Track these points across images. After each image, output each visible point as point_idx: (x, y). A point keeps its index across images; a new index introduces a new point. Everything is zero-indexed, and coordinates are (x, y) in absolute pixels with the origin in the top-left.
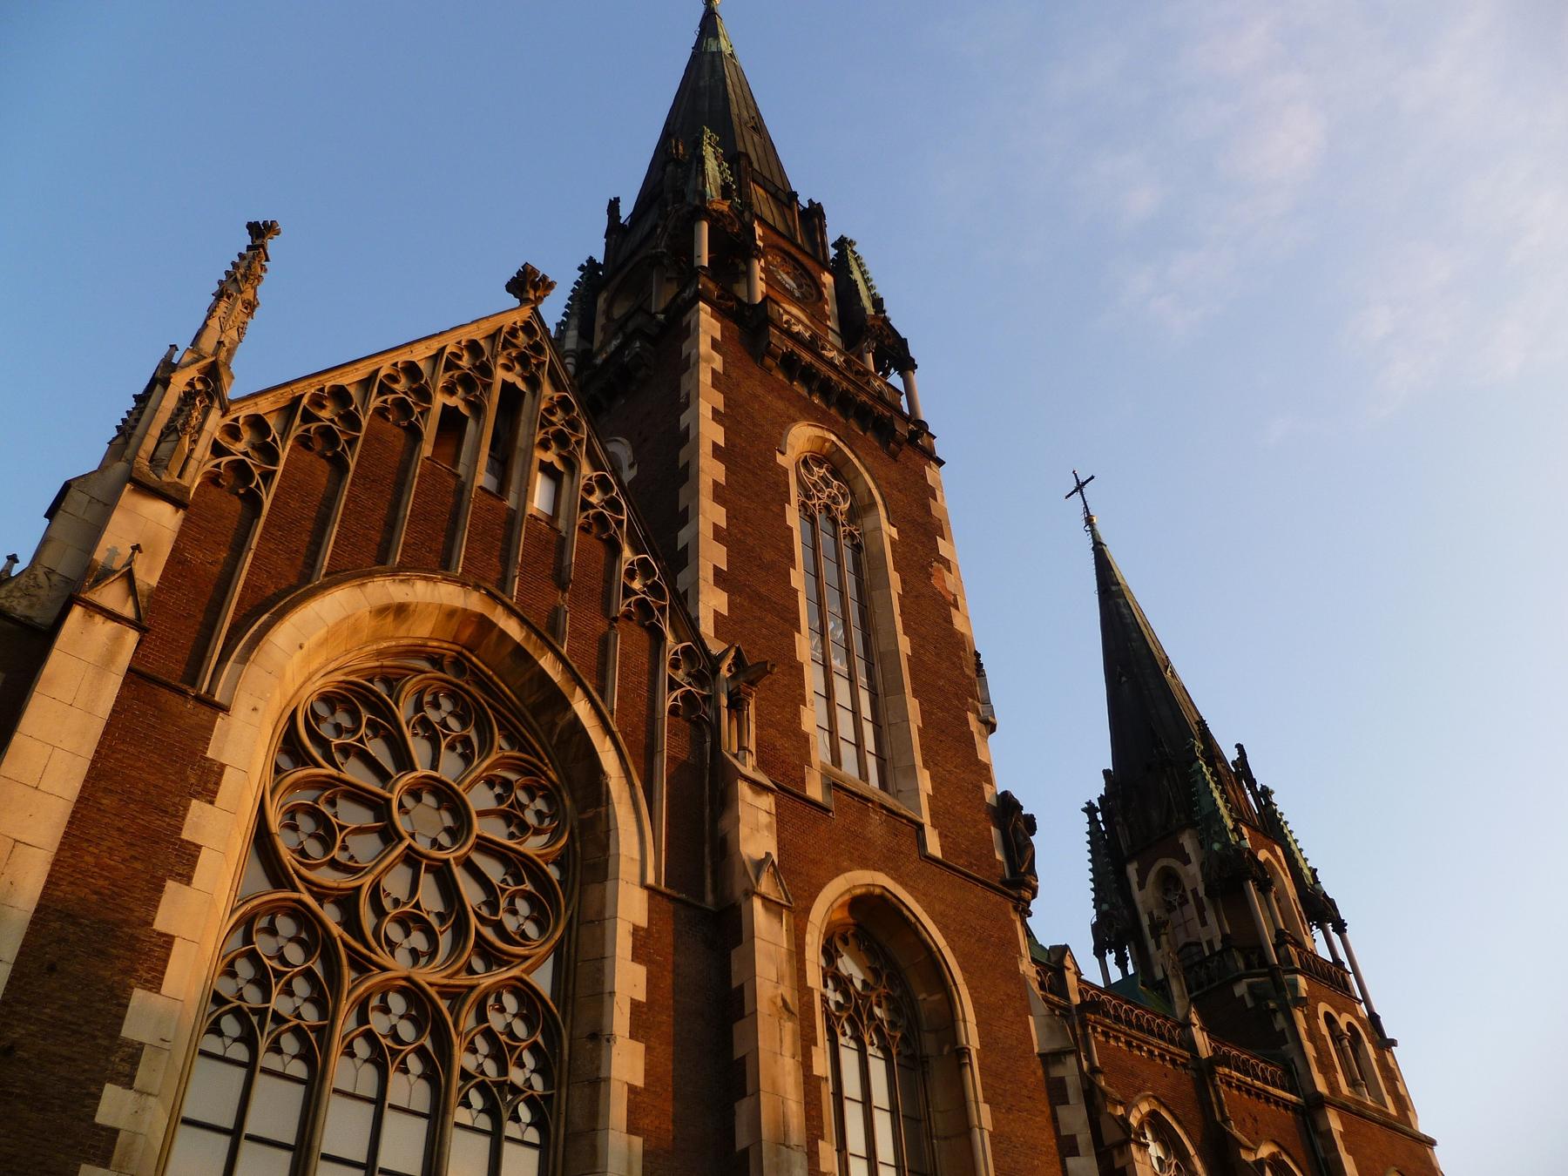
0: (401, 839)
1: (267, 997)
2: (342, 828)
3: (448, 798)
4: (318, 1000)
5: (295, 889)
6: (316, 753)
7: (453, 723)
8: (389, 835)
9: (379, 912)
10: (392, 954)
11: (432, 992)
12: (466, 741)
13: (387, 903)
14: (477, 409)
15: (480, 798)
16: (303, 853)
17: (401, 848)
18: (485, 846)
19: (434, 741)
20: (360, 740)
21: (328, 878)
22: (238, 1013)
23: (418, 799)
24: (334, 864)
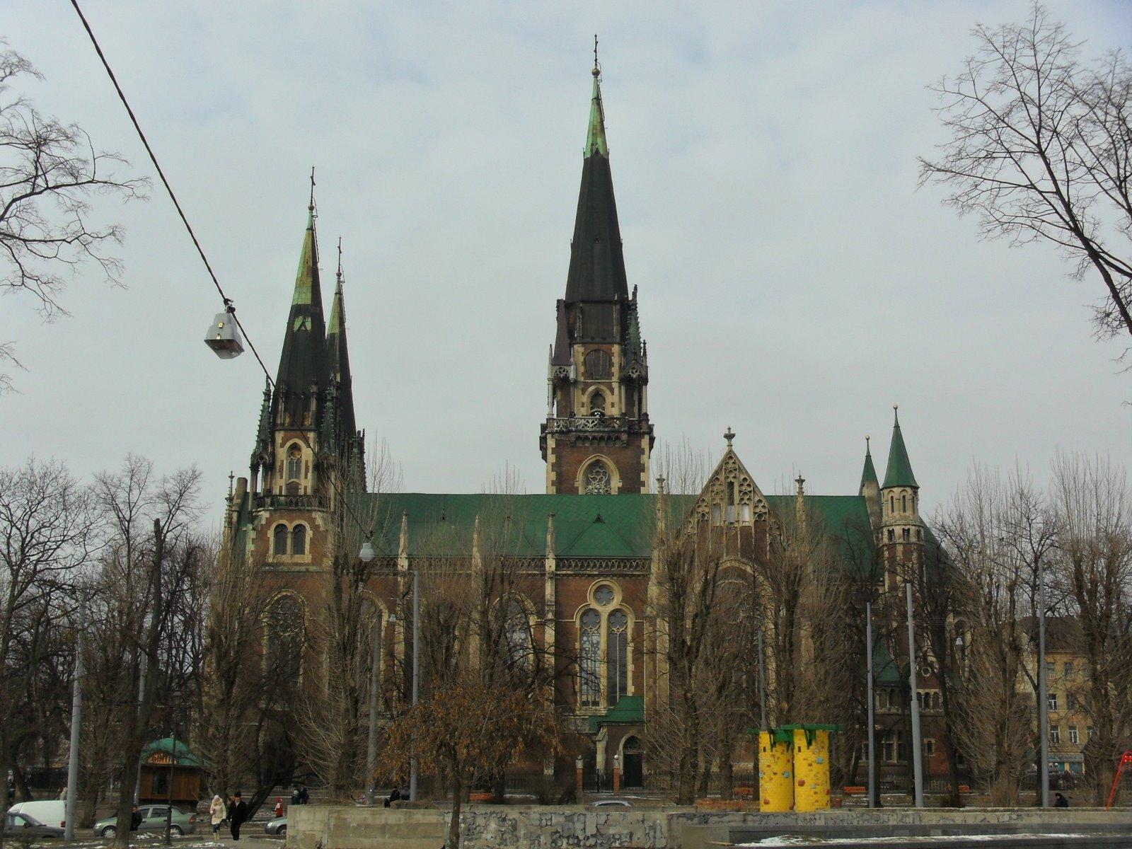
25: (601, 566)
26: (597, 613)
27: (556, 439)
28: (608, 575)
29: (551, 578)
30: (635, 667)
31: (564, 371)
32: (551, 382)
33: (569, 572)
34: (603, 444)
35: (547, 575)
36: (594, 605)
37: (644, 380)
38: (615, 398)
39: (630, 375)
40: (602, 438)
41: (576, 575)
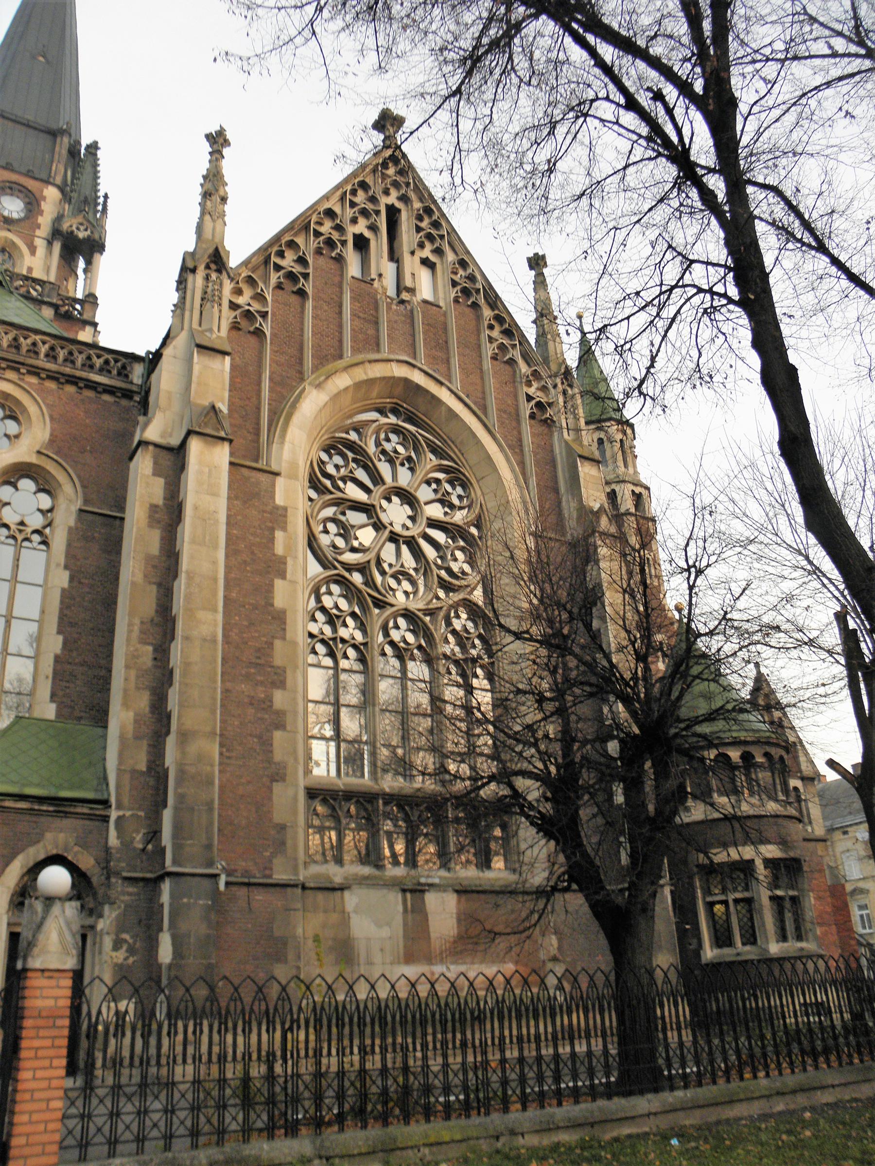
0: (385, 527)
1: (335, 630)
2: (353, 527)
3: (407, 497)
4: (362, 627)
5: (336, 568)
6: (328, 483)
7: (400, 449)
9: (383, 573)
10: (394, 595)
11: (420, 614)
12: (409, 459)
13: (386, 566)
14: (373, 228)
15: (424, 493)
16: (334, 546)
18: (433, 523)
19: (391, 461)
20: (351, 472)
21: (350, 557)
22: (323, 642)
23: (389, 500)
24: (354, 550)
30: (65, 643)
39: (72, 232)
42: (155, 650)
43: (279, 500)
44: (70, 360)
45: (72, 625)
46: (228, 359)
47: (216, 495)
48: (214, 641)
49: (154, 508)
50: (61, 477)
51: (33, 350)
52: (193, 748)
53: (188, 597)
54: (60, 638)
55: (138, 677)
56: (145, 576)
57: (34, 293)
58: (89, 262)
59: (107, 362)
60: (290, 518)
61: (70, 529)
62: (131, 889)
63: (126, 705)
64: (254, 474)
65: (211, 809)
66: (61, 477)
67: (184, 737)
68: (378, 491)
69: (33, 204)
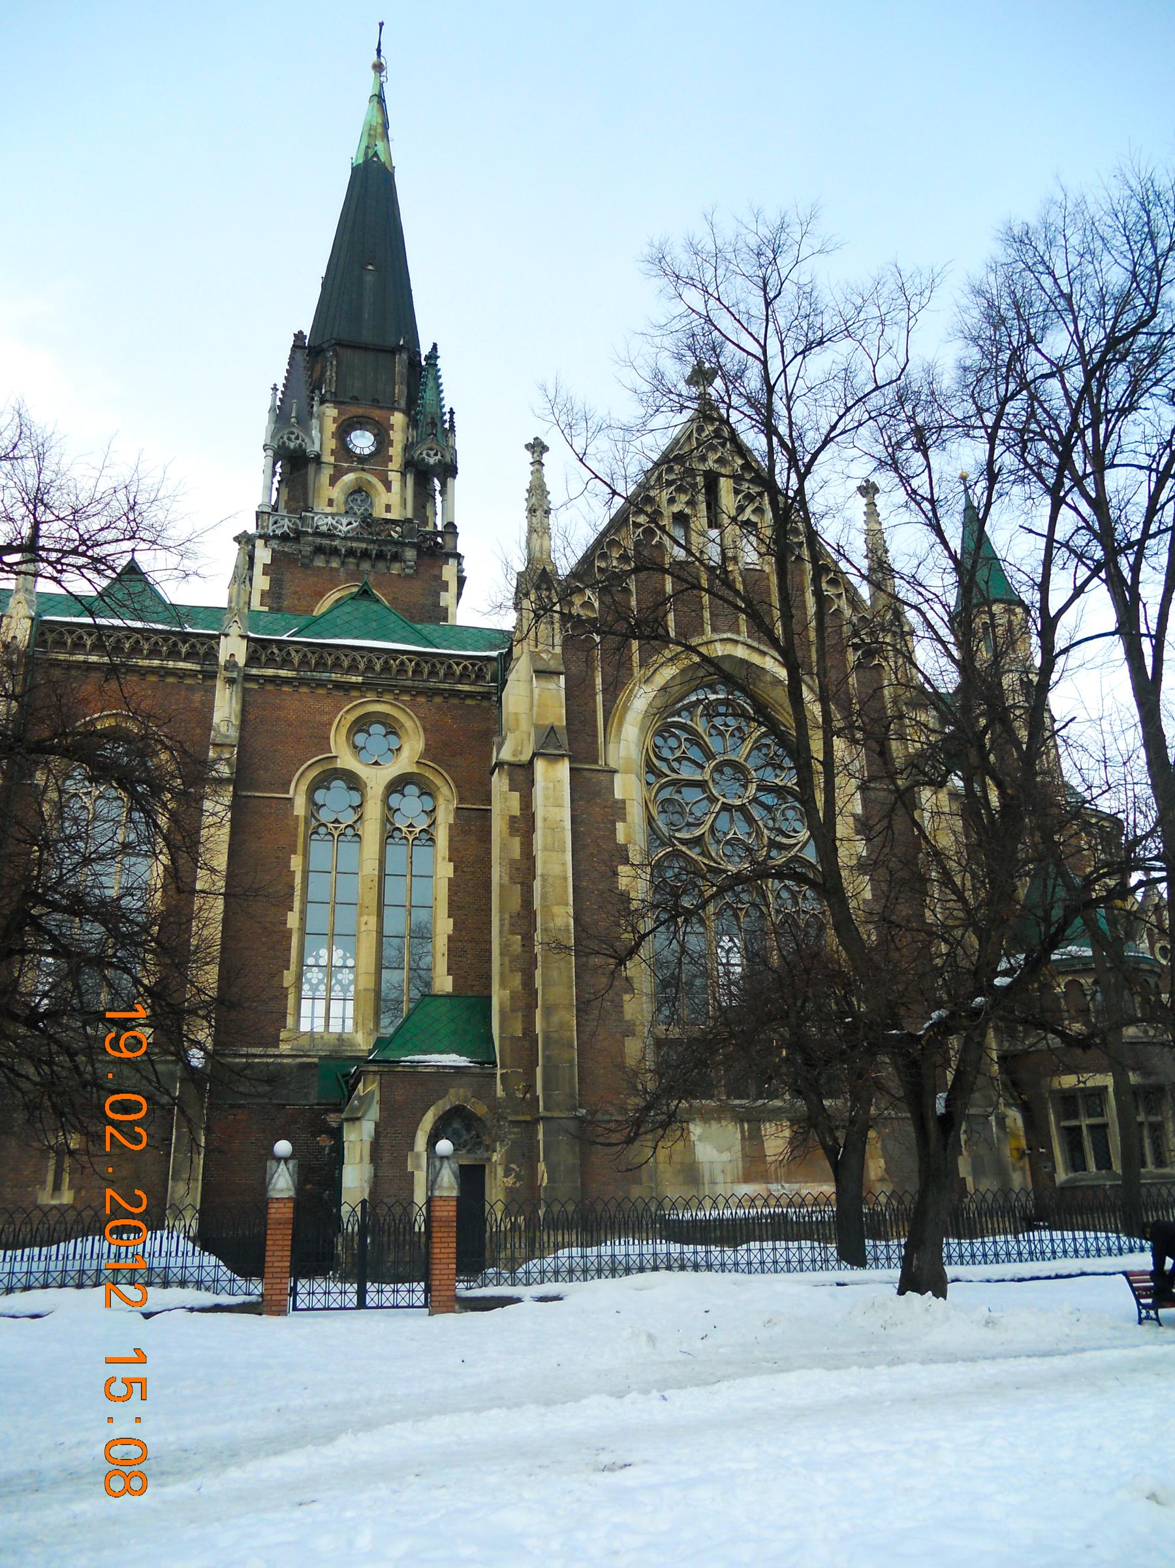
2: (687, 804)
8: (713, 800)
17: (720, 803)
25: (370, 667)
26: (353, 782)
27: (273, 550)
28: (389, 689)
29: (231, 681)
31: (297, 438)
32: (270, 453)
33: (283, 673)
34: (366, 566)
35: (222, 674)
36: (347, 760)
37: (449, 470)
38: (394, 498)
39: (423, 459)
40: (365, 554)
41: (302, 682)
42: (523, 939)
43: (618, 795)
44: (433, 673)
45: (461, 908)
46: (562, 677)
47: (561, 806)
48: (568, 930)
49: (513, 819)
50: (438, 782)
51: (402, 669)
52: (555, 1019)
53: (544, 897)
54: (451, 920)
55: (511, 962)
56: (511, 878)
57: (395, 535)
58: (444, 485)
59: (465, 667)
60: (629, 809)
61: (450, 825)
62: (515, 1130)
63: (503, 985)
64: (594, 775)
65: (572, 1066)
66: (438, 782)
67: (548, 1011)
68: (710, 766)
69: (383, 441)
